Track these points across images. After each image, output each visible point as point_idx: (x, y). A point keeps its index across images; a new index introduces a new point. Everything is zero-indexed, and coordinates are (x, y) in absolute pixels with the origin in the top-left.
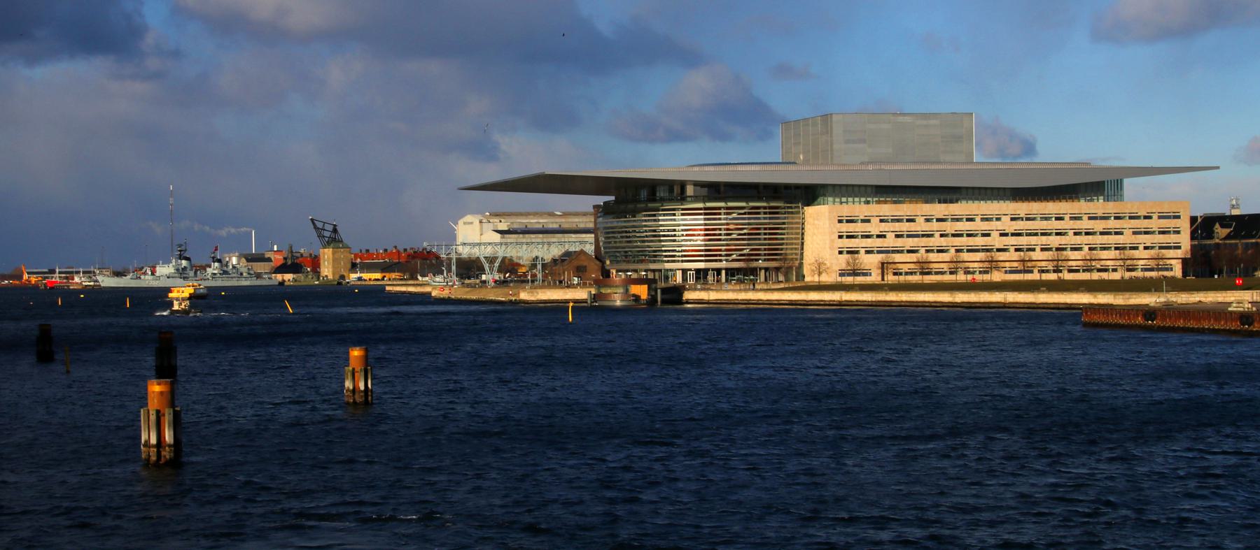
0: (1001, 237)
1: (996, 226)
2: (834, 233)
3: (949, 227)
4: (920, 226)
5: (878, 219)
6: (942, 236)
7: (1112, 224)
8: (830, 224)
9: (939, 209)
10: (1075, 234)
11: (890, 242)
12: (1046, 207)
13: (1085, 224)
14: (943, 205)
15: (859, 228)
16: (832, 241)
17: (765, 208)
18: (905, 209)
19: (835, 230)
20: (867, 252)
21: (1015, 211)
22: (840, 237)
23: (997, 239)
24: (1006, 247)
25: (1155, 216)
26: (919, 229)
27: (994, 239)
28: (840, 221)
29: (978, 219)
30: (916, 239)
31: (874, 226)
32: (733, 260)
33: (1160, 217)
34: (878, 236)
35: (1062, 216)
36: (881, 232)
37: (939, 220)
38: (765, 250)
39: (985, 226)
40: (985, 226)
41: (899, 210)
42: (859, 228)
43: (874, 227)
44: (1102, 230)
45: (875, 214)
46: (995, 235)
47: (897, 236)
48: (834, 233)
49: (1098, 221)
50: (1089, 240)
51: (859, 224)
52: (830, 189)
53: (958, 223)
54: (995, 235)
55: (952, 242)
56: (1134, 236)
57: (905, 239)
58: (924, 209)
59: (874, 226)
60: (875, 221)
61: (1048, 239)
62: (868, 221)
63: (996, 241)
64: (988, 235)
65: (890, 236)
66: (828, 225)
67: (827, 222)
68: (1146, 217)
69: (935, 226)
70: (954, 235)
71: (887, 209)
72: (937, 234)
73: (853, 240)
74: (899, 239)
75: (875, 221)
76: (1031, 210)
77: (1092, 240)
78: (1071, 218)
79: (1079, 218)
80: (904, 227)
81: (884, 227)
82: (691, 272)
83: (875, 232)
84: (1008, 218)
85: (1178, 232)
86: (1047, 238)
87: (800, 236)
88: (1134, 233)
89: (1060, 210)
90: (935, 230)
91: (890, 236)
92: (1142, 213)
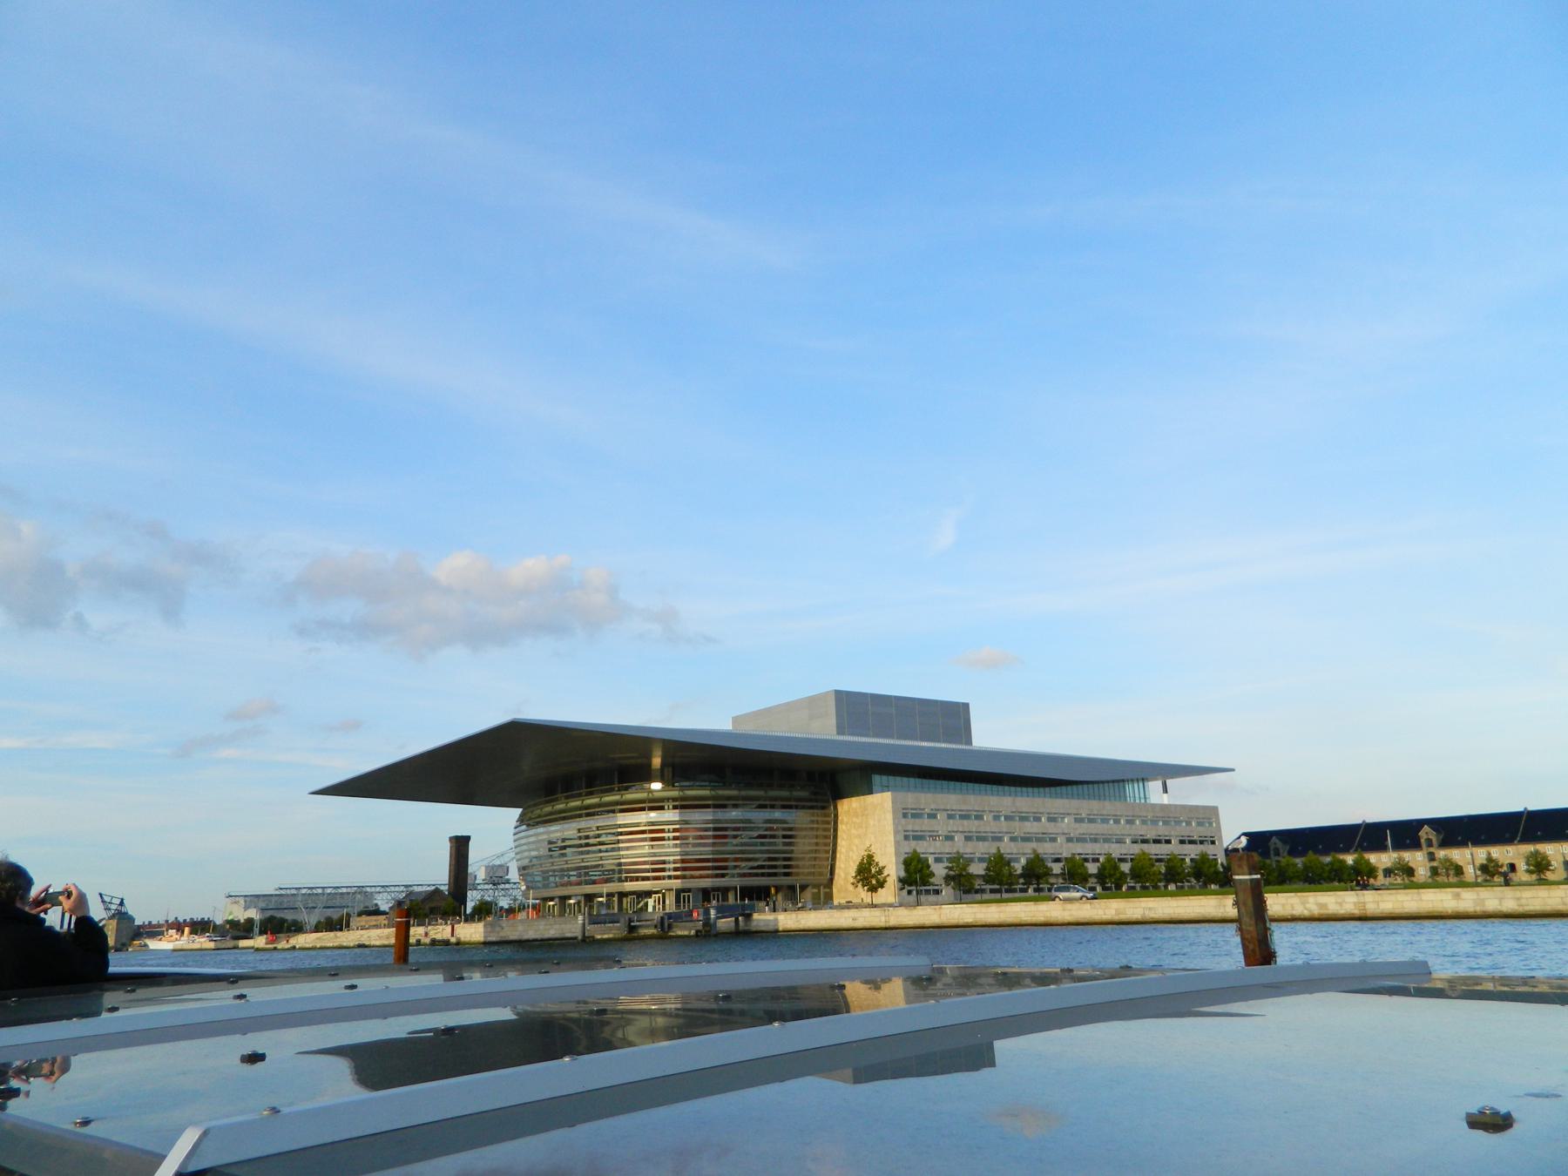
4: (988, 825)
5: (945, 814)
11: (959, 845)
15: (924, 825)
16: (897, 843)
17: (782, 799)
19: (900, 828)
23: (1064, 845)
26: (988, 830)
27: (1061, 846)
30: (986, 843)
32: (744, 875)
36: (949, 832)
37: (1007, 818)
40: (1051, 828)
42: (924, 825)
44: (1154, 838)
45: (942, 807)
58: (992, 803)
63: (1066, 850)
64: (1054, 840)
69: (1003, 825)
73: (920, 842)
74: (969, 843)
80: (972, 825)
81: (954, 825)
82: (686, 894)
85: (1213, 842)
88: (1182, 842)
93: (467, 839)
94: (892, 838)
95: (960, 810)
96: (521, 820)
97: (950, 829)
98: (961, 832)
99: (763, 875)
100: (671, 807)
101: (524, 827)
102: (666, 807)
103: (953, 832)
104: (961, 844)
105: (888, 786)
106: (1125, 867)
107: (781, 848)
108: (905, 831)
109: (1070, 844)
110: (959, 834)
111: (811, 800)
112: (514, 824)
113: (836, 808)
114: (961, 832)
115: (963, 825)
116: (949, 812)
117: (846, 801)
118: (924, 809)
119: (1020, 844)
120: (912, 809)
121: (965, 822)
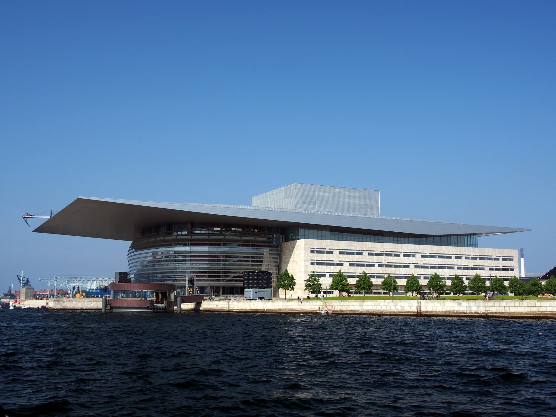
0: (415, 269)
1: (413, 261)
2: (308, 260)
3: (385, 260)
5: (338, 251)
6: (379, 266)
7: (478, 262)
8: (305, 253)
9: (377, 247)
10: (459, 268)
11: (346, 269)
12: (441, 249)
13: (463, 262)
15: (325, 257)
16: (306, 267)
17: (253, 241)
18: (356, 245)
19: (309, 258)
20: (330, 276)
21: (424, 250)
22: (312, 264)
24: (418, 276)
25: (501, 259)
27: (411, 270)
28: (312, 252)
29: (402, 255)
30: (363, 268)
31: (335, 257)
33: (503, 260)
34: (338, 264)
35: (450, 255)
36: (339, 261)
37: (377, 254)
39: (406, 260)
40: (406, 260)
41: (351, 246)
42: (325, 257)
43: (335, 257)
46: (412, 266)
47: (350, 265)
48: (308, 260)
49: (471, 260)
50: (466, 272)
51: (325, 255)
52: (302, 231)
53: (389, 257)
54: (412, 266)
55: (386, 271)
56: (490, 271)
57: (355, 267)
58: (368, 246)
59: (335, 257)
60: (336, 252)
61: (443, 271)
62: (331, 253)
63: (413, 271)
64: (408, 267)
65: (346, 264)
66: (303, 255)
67: (303, 252)
68: (497, 259)
69: (375, 258)
70: (387, 266)
71: (344, 245)
72: (376, 265)
73: (321, 266)
74: (352, 267)
75: (336, 252)
76: (433, 251)
77: (468, 273)
78: (456, 258)
79: (460, 258)
80: (355, 258)
83: (336, 261)
84: (419, 255)
86: (442, 270)
87: (278, 264)
88: (491, 269)
89: (449, 251)
90: (375, 261)
91: (346, 264)
92: (494, 256)
94: (303, 263)
95: (347, 250)
96: (132, 247)
97: (340, 260)
98: (347, 261)
99: (237, 281)
100: (190, 244)
101: (134, 250)
102: (187, 244)
103: (342, 261)
104: (347, 267)
105: (309, 236)
106: (449, 283)
108: (311, 260)
109: (417, 269)
110: (346, 262)
111: (267, 242)
113: (281, 246)
114: (347, 261)
115: (349, 258)
116: (340, 251)
118: (325, 249)
119: (384, 268)
120: (316, 248)
121: (350, 255)
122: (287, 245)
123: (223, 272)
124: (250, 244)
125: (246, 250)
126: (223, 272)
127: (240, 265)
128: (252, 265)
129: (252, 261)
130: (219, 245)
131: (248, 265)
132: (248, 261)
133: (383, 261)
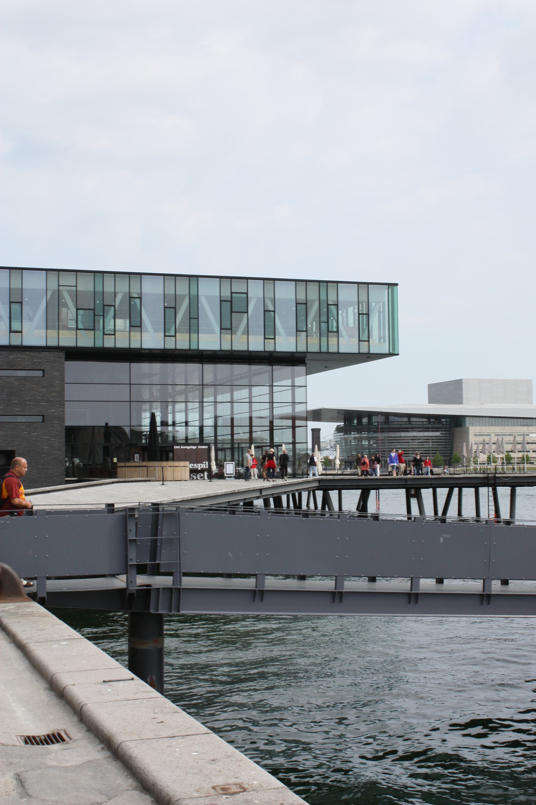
14: (526, 427)
17: (433, 428)
19: (473, 440)
28: (475, 435)
38: (432, 450)
52: (468, 420)
71: (498, 429)
93: (319, 430)
107: (431, 446)
112: (333, 432)
117: (457, 428)
122: (458, 430)
123: (412, 451)
124: (430, 430)
125: (426, 434)
126: (412, 451)
127: (423, 445)
128: (433, 445)
129: (432, 442)
130: (408, 431)
131: (429, 445)
132: (429, 442)
133: (529, 440)
